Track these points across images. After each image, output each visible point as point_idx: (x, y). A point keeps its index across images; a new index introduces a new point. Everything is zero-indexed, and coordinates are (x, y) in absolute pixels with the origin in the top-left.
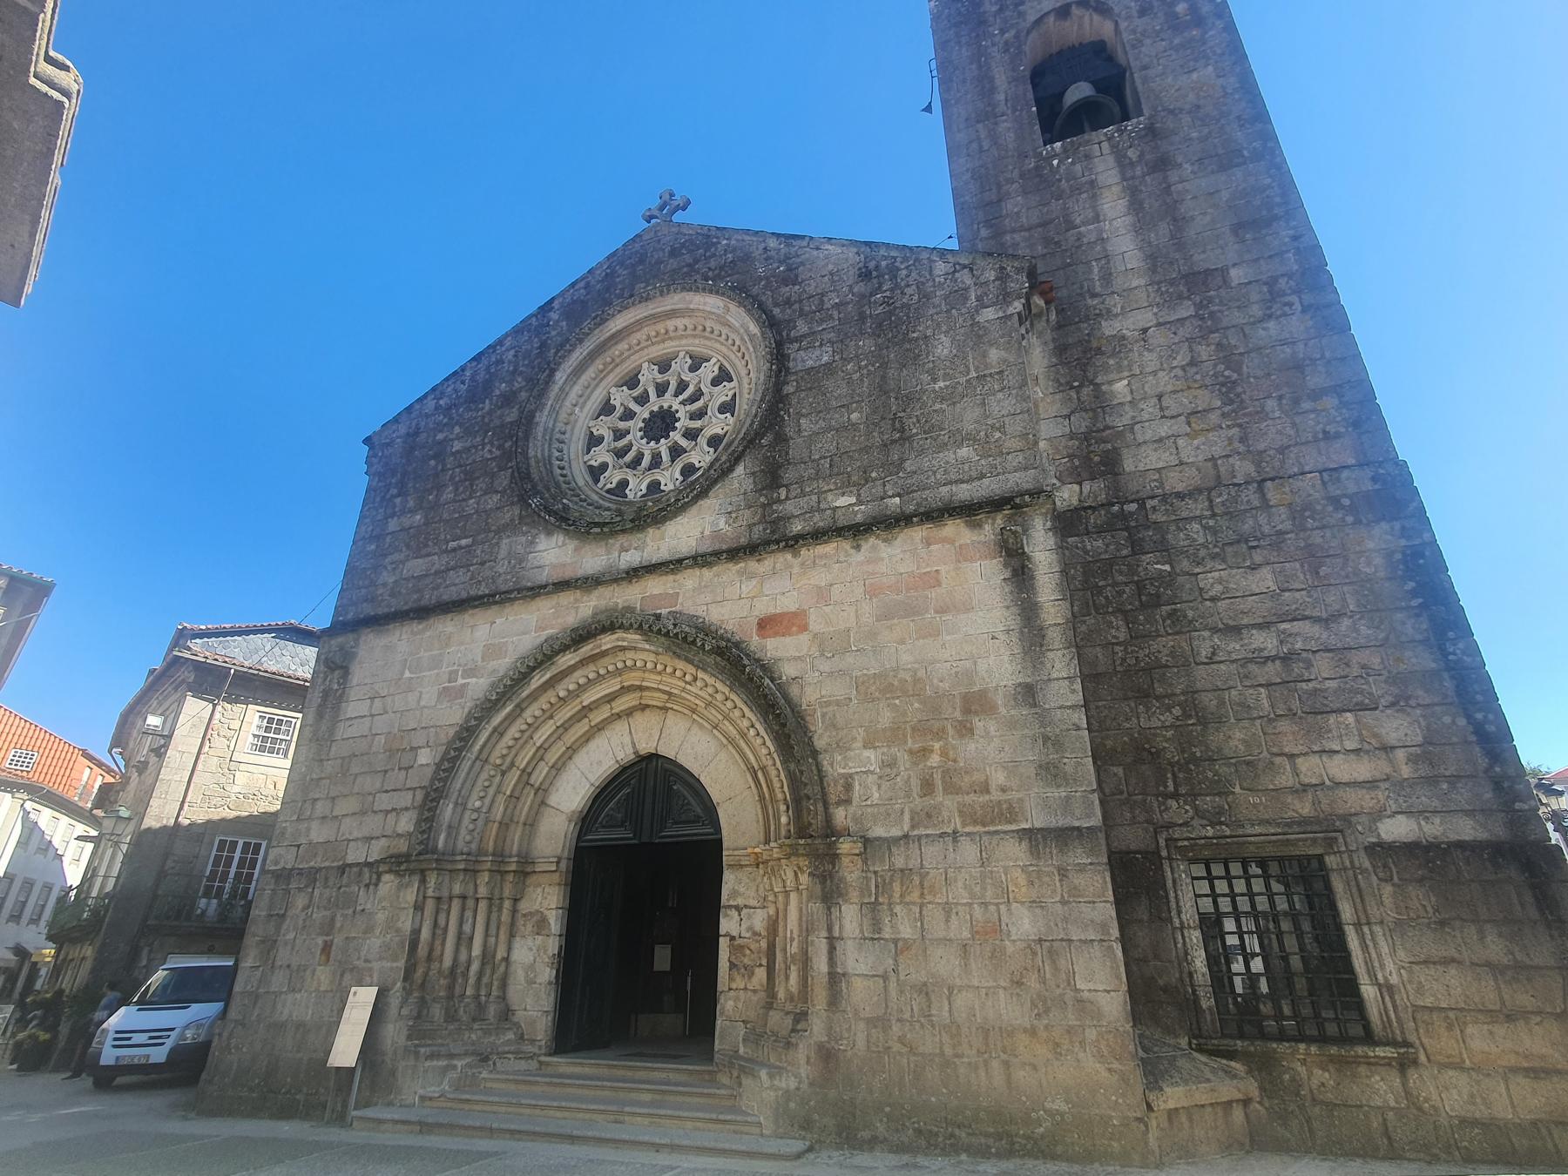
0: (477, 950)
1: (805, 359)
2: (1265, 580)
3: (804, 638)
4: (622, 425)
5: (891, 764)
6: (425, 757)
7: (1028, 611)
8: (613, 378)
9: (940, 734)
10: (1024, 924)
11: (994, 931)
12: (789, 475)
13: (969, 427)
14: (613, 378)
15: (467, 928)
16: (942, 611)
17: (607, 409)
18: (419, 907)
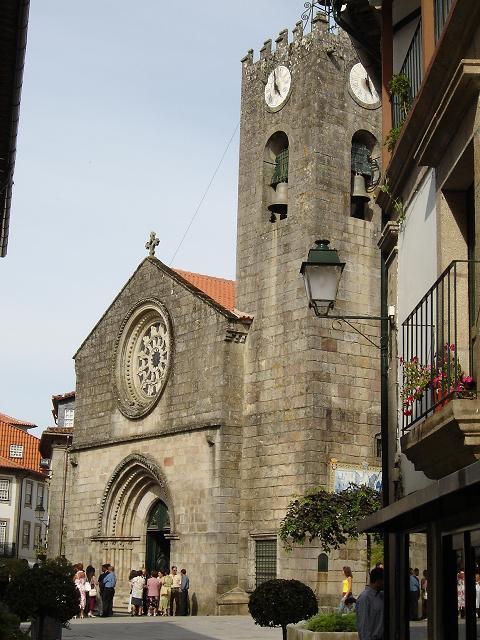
0: (121, 565)
1: (180, 347)
2: (279, 449)
3: (173, 467)
4: (146, 356)
5: (186, 512)
6: (99, 501)
7: (214, 462)
8: (143, 332)
9: (194, 503)
10: (203, 559)
11: (198, 560)
12: (175, 400)
13: (210, 389)
14: (143, 332)
15: (117, 558)
16: (199, 461)
17: (143, 347)
18: (101, 552)
